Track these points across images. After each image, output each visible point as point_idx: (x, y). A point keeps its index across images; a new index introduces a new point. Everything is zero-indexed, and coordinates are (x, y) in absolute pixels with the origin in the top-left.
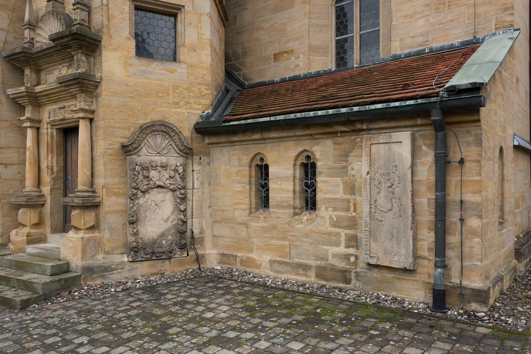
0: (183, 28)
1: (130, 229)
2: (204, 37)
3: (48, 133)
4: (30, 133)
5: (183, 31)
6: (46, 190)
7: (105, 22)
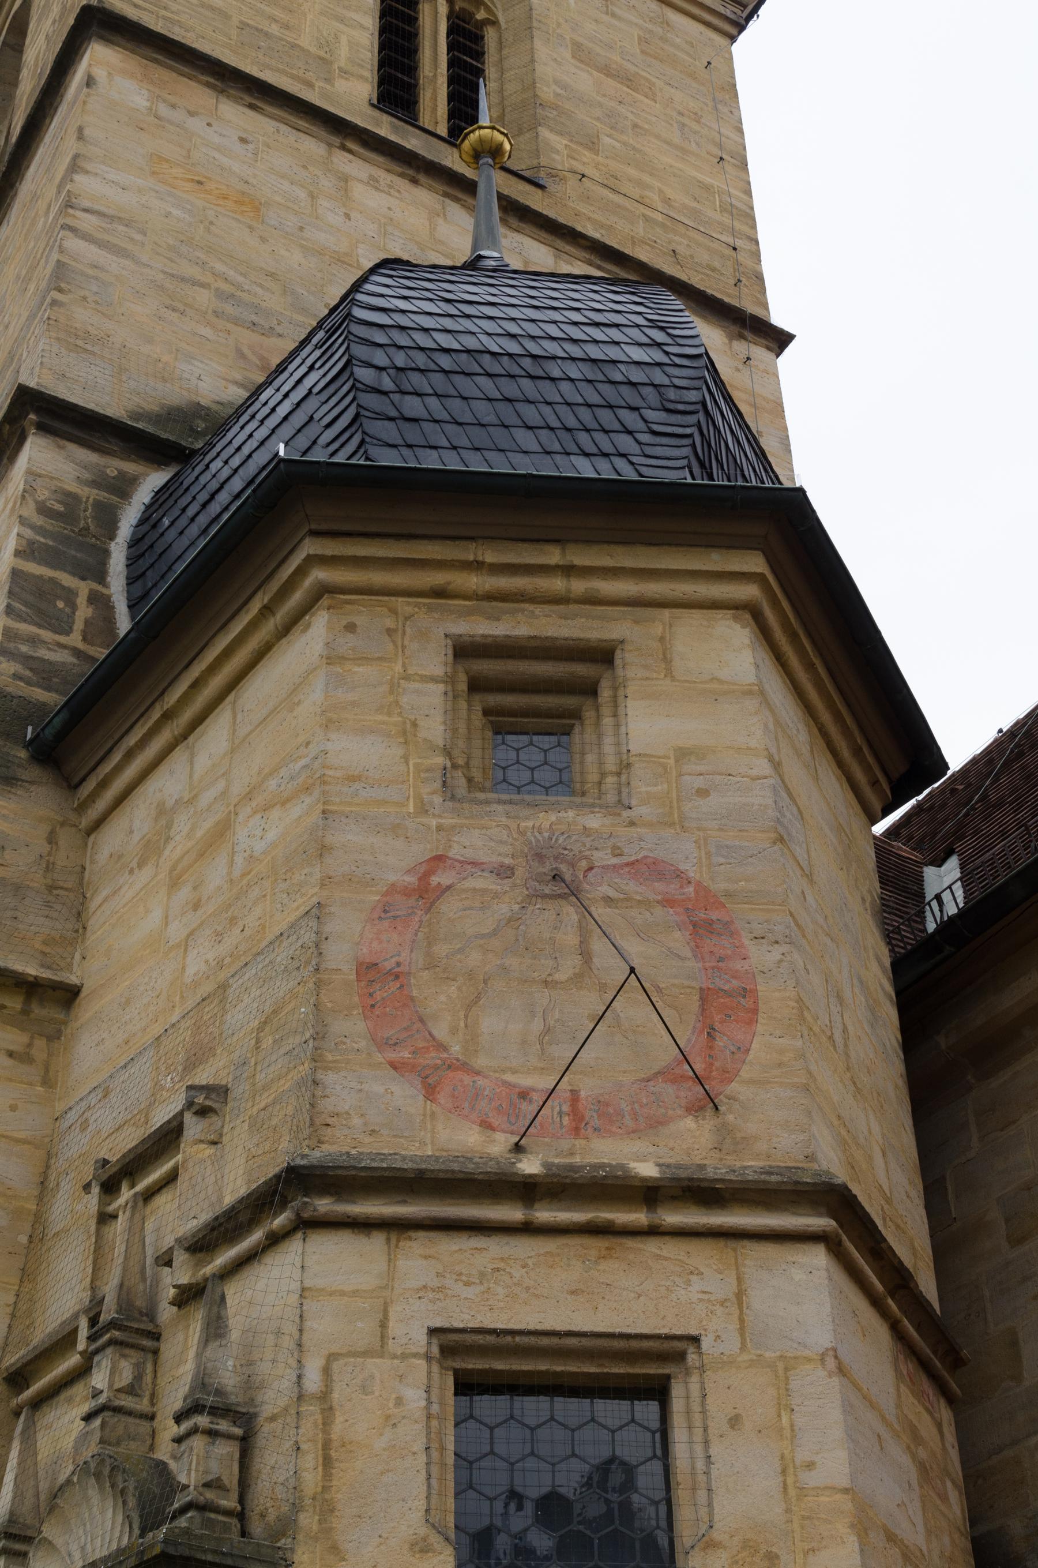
0: (699, 1449)
2: (813, 1479)
5: (700, 1465)
7: (311, 1480)
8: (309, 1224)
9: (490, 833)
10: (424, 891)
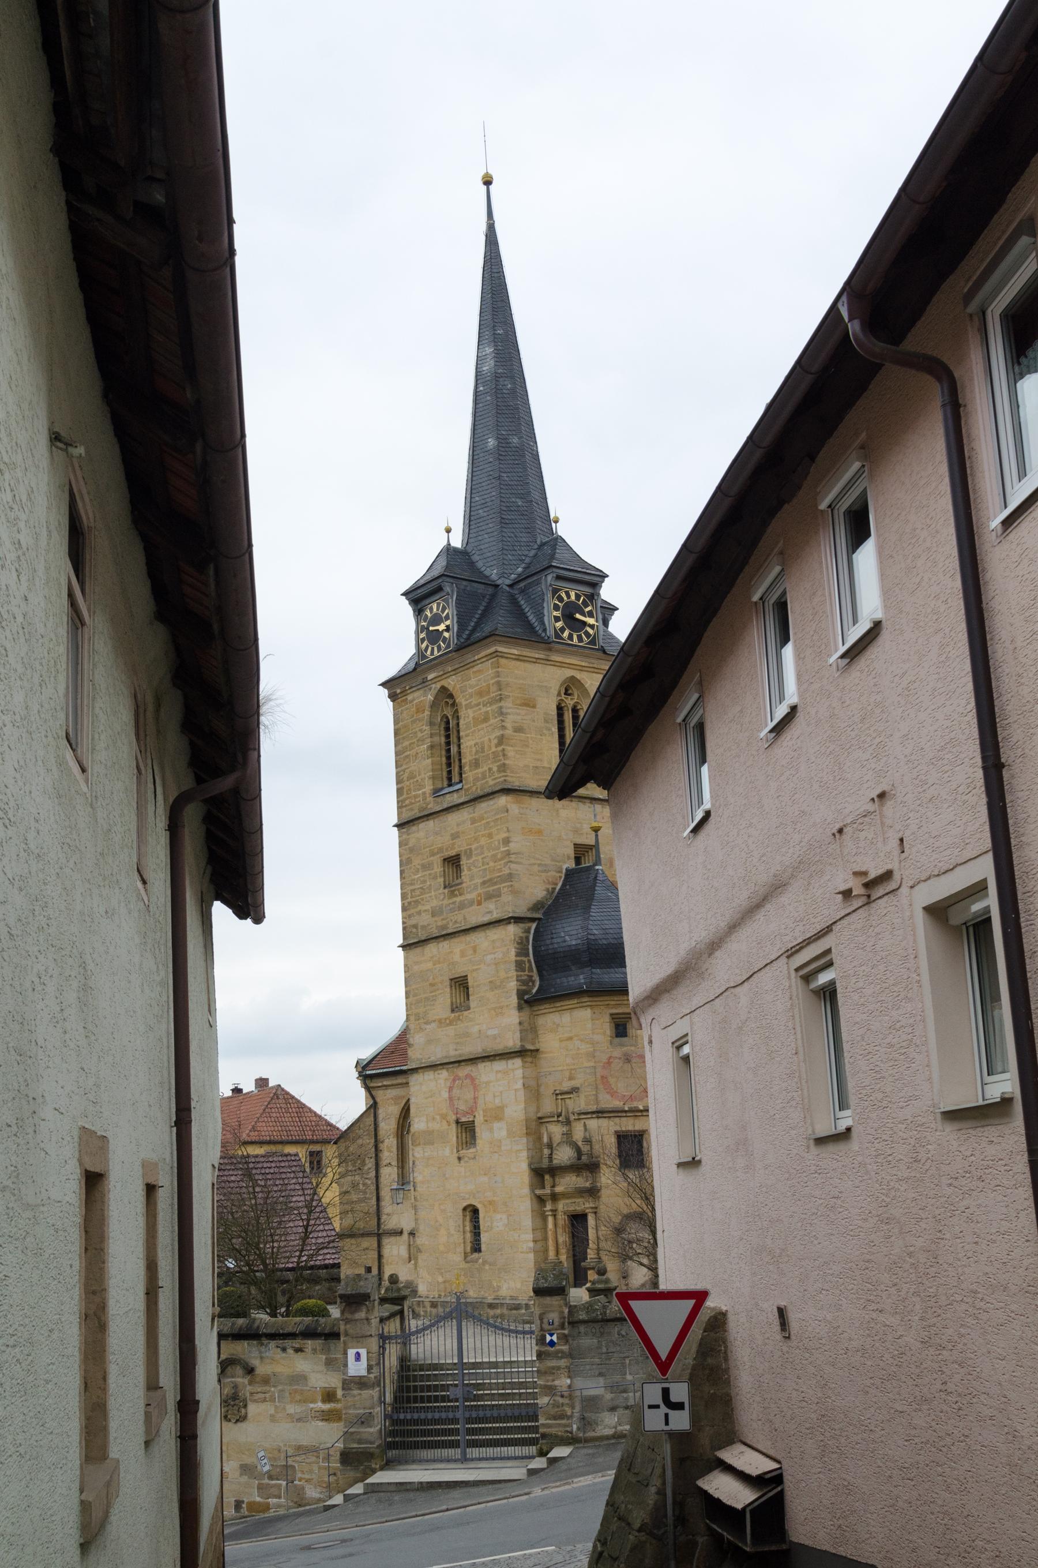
1: (623, 1282)
3: (562, 1219)
4: (550, 1219)
6: (563, 1258)
8: (598, 1117)
9: (617, 1052)
10: (609, 1063)
